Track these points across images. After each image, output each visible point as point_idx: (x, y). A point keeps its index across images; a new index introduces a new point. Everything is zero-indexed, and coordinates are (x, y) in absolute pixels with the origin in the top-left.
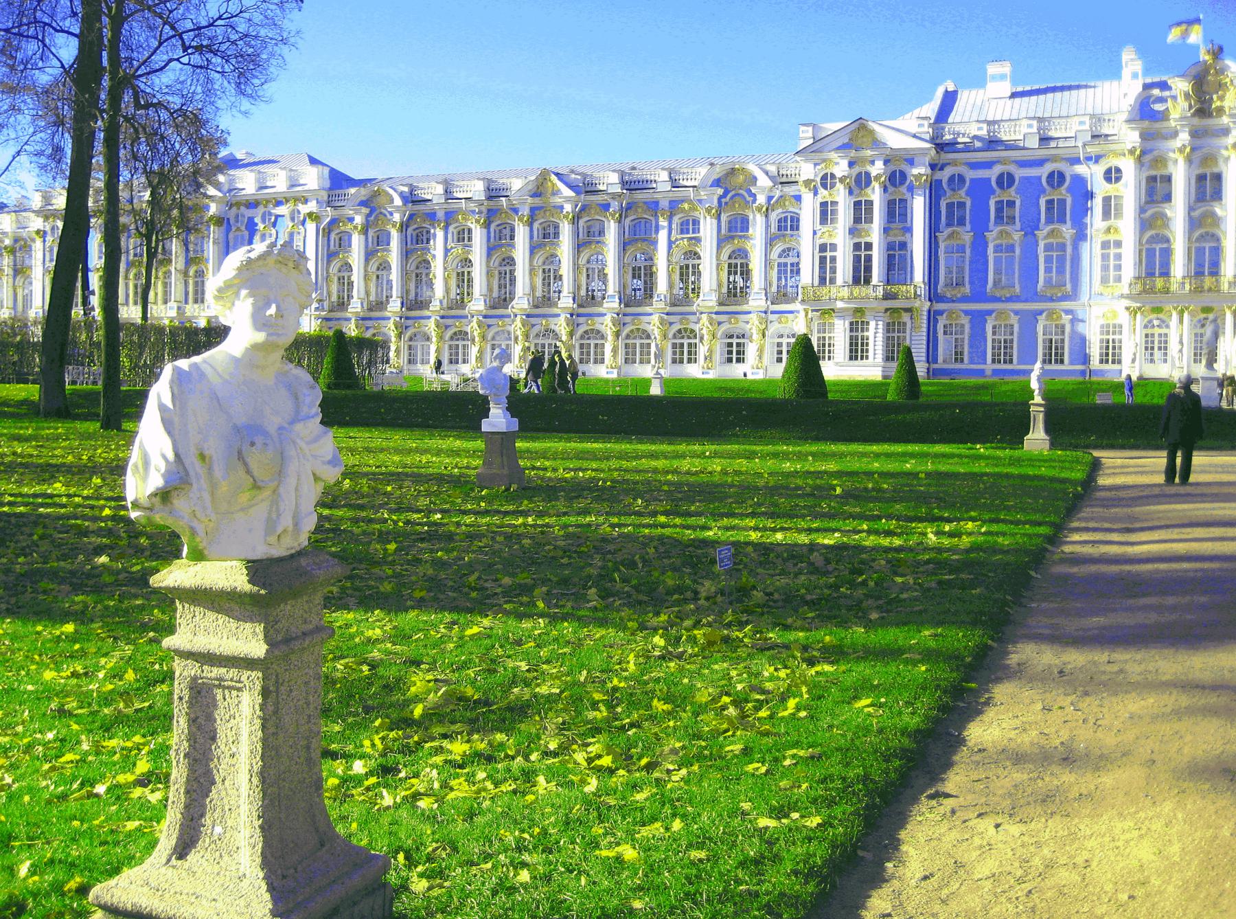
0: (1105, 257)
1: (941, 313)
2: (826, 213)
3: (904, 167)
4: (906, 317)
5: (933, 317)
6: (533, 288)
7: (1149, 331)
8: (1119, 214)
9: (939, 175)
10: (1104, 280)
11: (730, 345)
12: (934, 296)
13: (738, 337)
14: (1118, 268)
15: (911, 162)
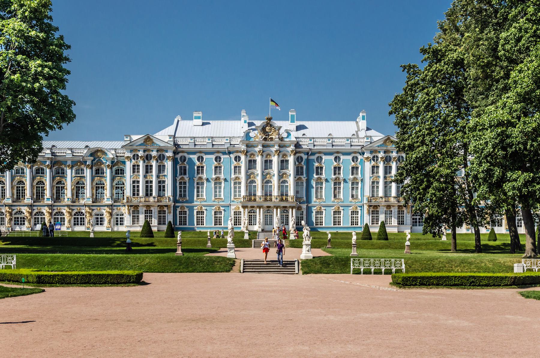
0: (235, 188)
1: (178, 207)
2: (135, 168)
3: (164, 153)
4: (166, 209)
5: (175, 208)
6: (13, 194)
7: (250, 214)
8: (240, 173)
9: (176, 156)
10: (235, 196)
11: (97, 218)
12: (175, 201)
13: (101, 215)
14: (240, 192)
15: (167, 152)
